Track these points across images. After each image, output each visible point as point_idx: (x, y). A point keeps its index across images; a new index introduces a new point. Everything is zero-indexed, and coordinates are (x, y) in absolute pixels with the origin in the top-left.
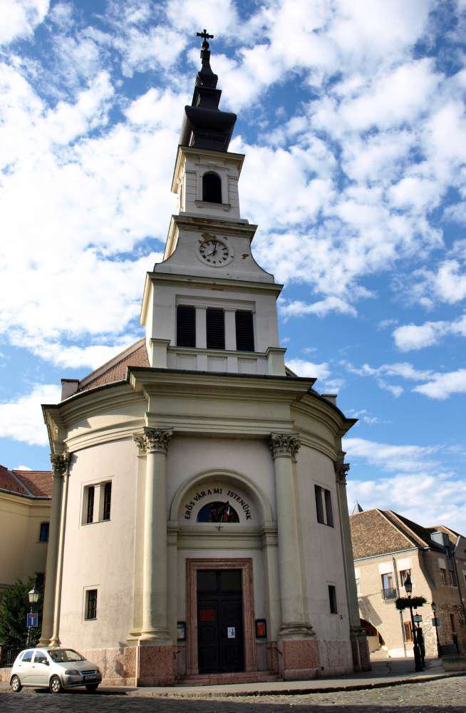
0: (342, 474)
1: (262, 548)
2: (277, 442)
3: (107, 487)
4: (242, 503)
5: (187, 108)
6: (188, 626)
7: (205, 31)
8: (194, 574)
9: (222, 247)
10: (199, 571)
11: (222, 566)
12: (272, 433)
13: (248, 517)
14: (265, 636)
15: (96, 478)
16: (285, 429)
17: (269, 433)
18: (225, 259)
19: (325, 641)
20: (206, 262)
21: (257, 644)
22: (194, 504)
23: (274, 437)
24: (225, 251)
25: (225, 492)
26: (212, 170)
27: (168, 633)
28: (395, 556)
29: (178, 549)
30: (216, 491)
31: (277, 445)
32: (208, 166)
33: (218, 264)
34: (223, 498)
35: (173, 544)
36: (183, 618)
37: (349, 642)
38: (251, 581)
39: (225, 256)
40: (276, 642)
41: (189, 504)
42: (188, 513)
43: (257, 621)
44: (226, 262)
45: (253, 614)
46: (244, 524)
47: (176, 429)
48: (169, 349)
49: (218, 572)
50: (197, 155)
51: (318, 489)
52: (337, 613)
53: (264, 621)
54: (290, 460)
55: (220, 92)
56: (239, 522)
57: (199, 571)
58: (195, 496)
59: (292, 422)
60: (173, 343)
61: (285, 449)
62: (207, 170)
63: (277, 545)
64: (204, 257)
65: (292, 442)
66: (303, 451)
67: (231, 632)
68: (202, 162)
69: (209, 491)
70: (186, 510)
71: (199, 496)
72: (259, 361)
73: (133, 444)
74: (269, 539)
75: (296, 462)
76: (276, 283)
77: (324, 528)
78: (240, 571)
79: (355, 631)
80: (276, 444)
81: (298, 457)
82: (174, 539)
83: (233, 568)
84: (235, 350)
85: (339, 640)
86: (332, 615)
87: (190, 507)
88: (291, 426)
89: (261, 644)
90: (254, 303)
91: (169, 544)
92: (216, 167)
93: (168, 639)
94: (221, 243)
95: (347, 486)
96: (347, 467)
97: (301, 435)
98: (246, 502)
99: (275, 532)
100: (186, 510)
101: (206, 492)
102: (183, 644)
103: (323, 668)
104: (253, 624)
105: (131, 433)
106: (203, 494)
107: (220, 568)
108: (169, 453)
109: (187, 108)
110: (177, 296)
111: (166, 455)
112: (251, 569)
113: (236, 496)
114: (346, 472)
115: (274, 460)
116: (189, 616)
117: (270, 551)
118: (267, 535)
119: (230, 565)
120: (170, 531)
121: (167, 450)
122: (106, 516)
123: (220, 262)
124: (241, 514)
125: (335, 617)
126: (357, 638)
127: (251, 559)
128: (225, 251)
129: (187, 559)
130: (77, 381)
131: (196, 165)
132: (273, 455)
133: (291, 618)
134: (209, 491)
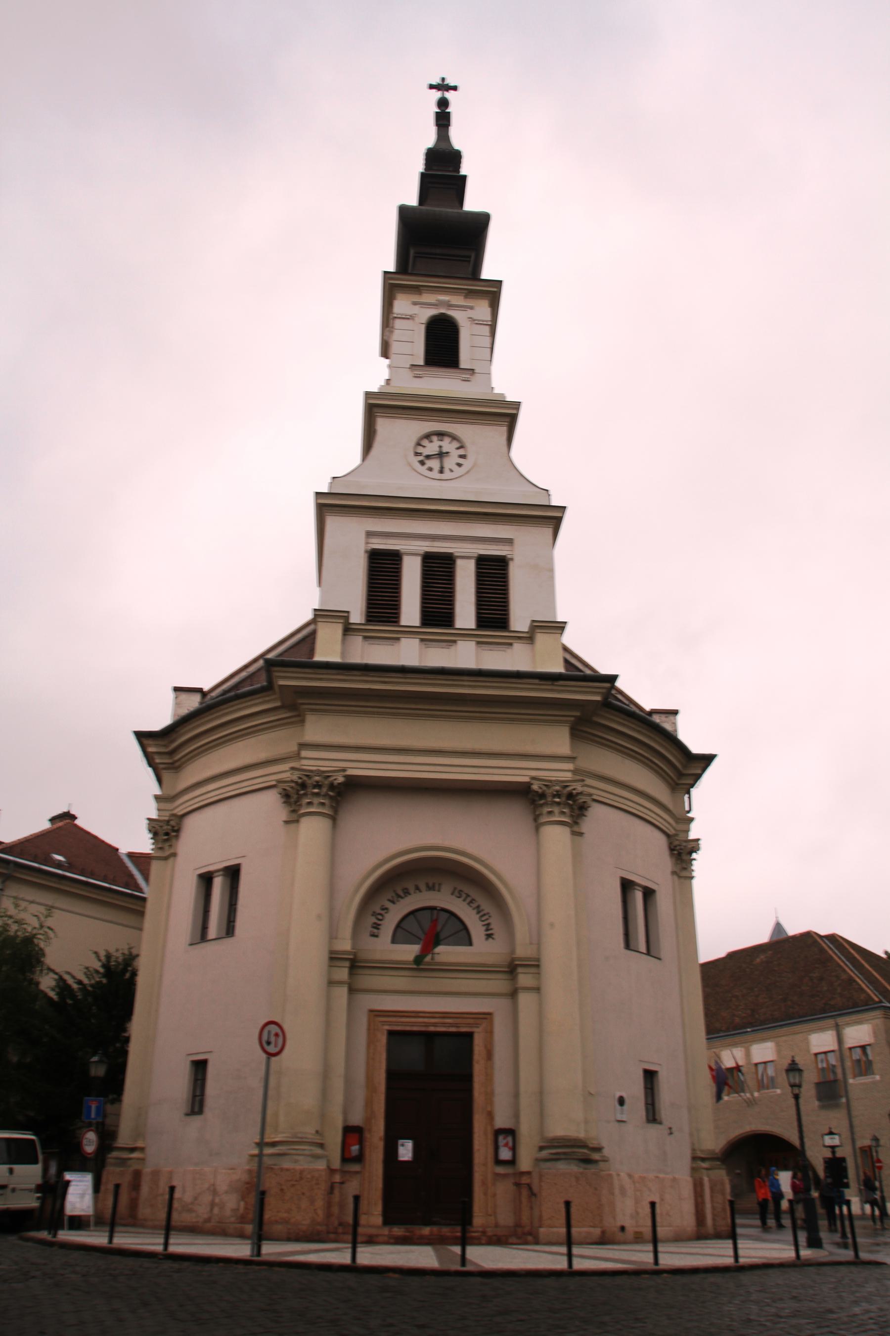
0: (685, 857)
1: (513, 994)
2: (543, 796)
3: (233, 873)
4: (478, 909)
5: (404, 212)
8: (383, 1039)
9: (456, 444)
10: (391, 1033)
11: (435, 1025)
12: (534, 778)
13: (489, 936)
14: (512, 1162)
15: (216, 861)
16: (561, 772)
17: (527, 779)
18: (459, 465)
19: (630, 1176)
21: (497, 1175)
22: (386, 909)
23: (535, 787)
24: (461, 452)
26: (443, 311)
27: (321, 1146)
28: (841, 1020)
29: (352, 990)
30: (430, 888)
31: (542, 802)
33: (447, 475)
35: (340, 983)
36: (356, 1119)
37: (689, 1179)
38: (489, 1055)
39: (461, 461)
40: (529, 1173)
42: (376, 926)
43: (499, 1132)
45: (490, 1115)
47: (350, 772)
48: (348, 629)
49: (429, 1037)
51: (627, 886)
52: (660, 1123)
53: (511, 1132)
54: (567, 830)
55: (464, 178)
56: (470, 943)
57: (391, 1033)
59: (571, 759)
60: (357, 617)
61: (556, 810)
63: (537, 989)
64: (422, 463)
65: (570, 796)
66: (596, 812)
67: (406, 1151)
70: (374, 920)
73: (271, 801)
74: (524, 979)
75: (581, 834)
76: (554, 503)
77: (640, 963)
78: (470, 1036)
79: (703, 1159)
80: (541, 799)
81: (587, 825)
82: (343, 973)
85: (661, 1175)
86: (650, 1125)
87: (380, 916)
88: (570, 766)
89: (505, 1176)
90: (509, 541)
91: (331, 983)
92: (450, 306)
93: (316, 1157)
94: (454, 438)
95: (695, 882)
96: (694, 846)
97: (589, 781)
98: (486, 906)
99: (535, 965)
100: (374, 920)
101: (412, 889)
102: (355, 1167)
103: (623, 1228)
104: (490, 1136)
105: (272, 780)
106: (407, 892)
107: (432, 1029)
109: (404, 212)
110: (370, 534)
111: (334, 819)
112: (490, 1032)
113: (468, 896)
114: (694, 855)
115: (537, 828)
116: (370, 1117)
117: (524, 999)
118: (520, 970)
119: (451, 1025)
120: (334, 958)
121: (336, 810)
122: (229, 929)
123: (451, 471)
124: (476, 929)
125: (653, 1131)
126: (705, 1172)
127: (490, 1014)
128: (461, 452)
129: (371, 1011)
130: (199, 690)
131: (415, 304)
132: (536, 819)
133: (559, 1129)
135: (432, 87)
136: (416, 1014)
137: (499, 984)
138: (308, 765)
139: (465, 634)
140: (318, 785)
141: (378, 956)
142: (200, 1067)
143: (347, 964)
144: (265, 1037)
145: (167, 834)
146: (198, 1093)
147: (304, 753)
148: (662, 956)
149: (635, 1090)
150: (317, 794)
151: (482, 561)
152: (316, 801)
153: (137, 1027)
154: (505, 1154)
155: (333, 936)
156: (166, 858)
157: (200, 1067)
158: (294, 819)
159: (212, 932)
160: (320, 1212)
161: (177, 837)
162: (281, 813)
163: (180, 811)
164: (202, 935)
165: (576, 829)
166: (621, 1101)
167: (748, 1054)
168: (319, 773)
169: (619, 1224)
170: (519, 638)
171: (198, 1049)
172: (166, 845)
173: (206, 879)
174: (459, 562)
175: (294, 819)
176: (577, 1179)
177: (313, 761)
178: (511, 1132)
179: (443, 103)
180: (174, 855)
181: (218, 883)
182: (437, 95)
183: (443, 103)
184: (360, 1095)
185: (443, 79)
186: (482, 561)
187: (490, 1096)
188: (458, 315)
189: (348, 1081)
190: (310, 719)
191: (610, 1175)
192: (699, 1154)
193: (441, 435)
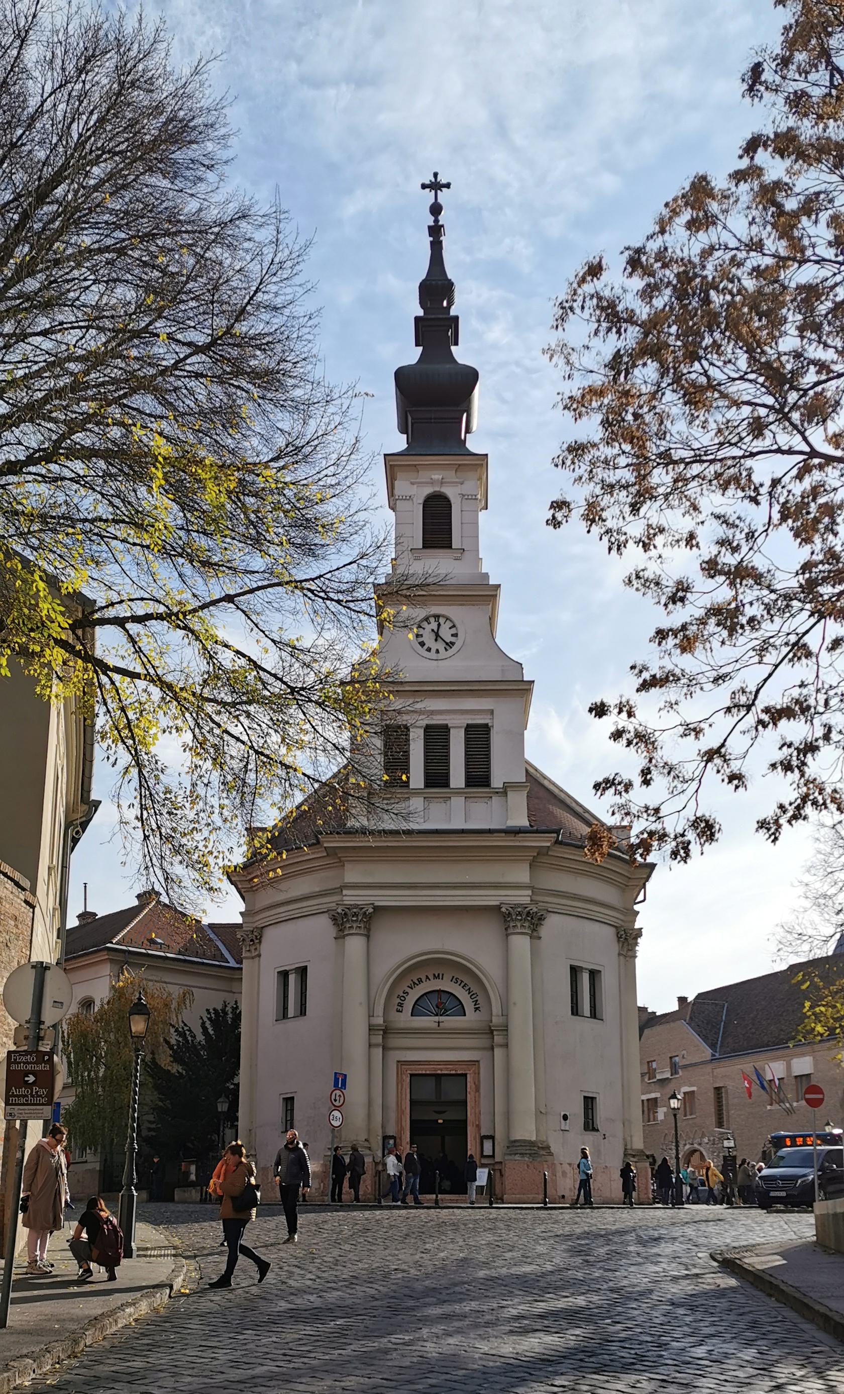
3: (303, 972)
6: (398, 1140)
7: (436, 175)
9: (449, 624)
10: (411, 1075)
13: (476, 1009)
15: (290, 963)
16: (523, 897)
17: (497, 903)
19: (570, 1164)
20: (426, 654)
24: (453, 631)
25: (447, 977)
26: (437, 489)
32: (432, 483)
34: (446, 985)
35: (377, 1045)
36: (391, 1132)
38: (477, 1089)
41: (402, 994)
42: (400, 1005)
43: (483, 1138)
44: (451, 652)
45: (478, 1127)
46: (471, 1018)
47: (377, 904)
50: (415, 465)
51: (575, 971)
52: (598, 1130)
58: (409, 983)
62: (428, 490)
63: (506, 1046)
65: (528, 913)
68: (424, 476)
69: (427, 977)
71: (414, 983)
72: (495, 799)
73: (324, 924)
74: (498, 1039)
78: (465, 1075)
81: (545, 931)
82: (379, 1039)
83: (454, 1072)
84: (463, 786)
87: (402, 998)
99: (505, 1029)
101: (424, 980)
105: (324, 908)
106: (420, 981)
107: (439, 1072)
108: (371, 933)
109: (402, 376)
111: (368, 936)
115: (507, 935)
116: (401, 1129)
117: (498, 1052)
120: (371, 1029)
121: (369, 930)
122: (302, 1011)
128: (453, 631)
129: (398, 1062)
131: (412, 484)
134: (427, 977)
135: (424, 186)
136: (428, 1063)
137: (484, 1042)
138: (348, 901)
139: (458, 792)
140: (355, 915)
141: (402, 1025)
142: (289, 1102)
143: (381, 1032)
144: (333, 1097)
145: (252, 940)
146: (289, 1118)
147: (345, 892)
148: (604, 1018)
149: (577, 1109)
150: (356, 921)
151: (469, 728)
152: (355, 925)
153: (243, 1077)
154: (488, 1151)
155: (371, 1015)
156: (253, 958)
157: (289, 1102)
158: (341, 936)
159: (291, 1011)
160: (369, 1188)
161: (260, 942)
162: (332, 931)
163: (259, 924)
164: (284, 1015)
165: (535, 934)
166: (565, 1118)
167: (789, 1068)
168: (356, 906)
169: (561, 1194)
170: (497, 793)
171: (288, 1089)
172: (253, 948)
173: (284, 975)
174: (452, 731)
175: (341, 936)
176: (528, 1166)
177: (351, 898)
178: (492, 1138)
179: (436, 209)
180: (259, 956)
181: (292, 978)
182: (429, 195)
183: (436, 209)
184: (392, 1115)
185: (436, 175)
186: (469, 728)
187: (478, 1115)
188: (450, 492)
189: (384, 1107)
190: (348, 866)
191: (553, 1164)
192: (630, 1152)
193: (436, 617)
